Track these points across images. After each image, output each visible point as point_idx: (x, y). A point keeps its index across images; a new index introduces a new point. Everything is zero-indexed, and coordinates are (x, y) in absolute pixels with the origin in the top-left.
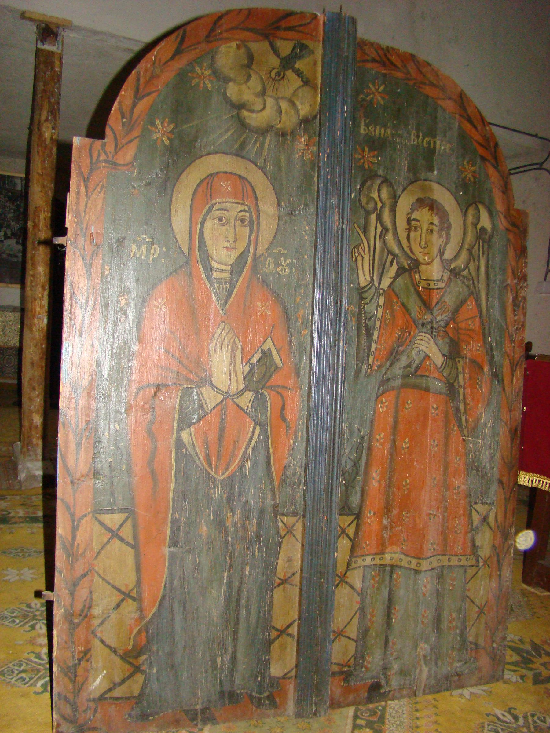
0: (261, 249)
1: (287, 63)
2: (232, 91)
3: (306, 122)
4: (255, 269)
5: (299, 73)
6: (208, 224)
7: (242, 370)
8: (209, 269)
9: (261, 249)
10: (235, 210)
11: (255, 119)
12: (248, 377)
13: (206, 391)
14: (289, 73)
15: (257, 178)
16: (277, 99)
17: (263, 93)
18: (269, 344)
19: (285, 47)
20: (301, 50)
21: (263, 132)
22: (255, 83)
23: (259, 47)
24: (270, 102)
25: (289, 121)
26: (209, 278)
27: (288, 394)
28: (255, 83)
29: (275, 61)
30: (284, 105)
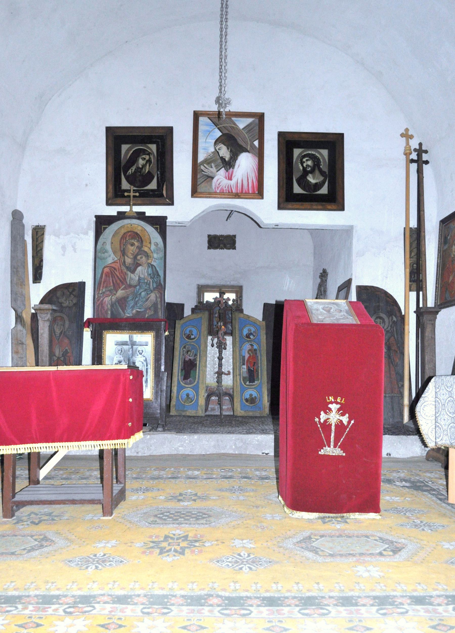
0: (66, 329)
1: (71, 293)
2: (60, 300)
3: (74, 304)
4: (64, 334)
5: (73, 295)
6: (55, 326)
7: (61, 353)
8: (55, 335)
9: (66, 329)
10: (60, 323)
11: (64, 305)
12: (63, 354)
13: (54, 357)
14: (72, 295)
15: (65, 317)
16: (69, 301)
17: (66, 300)
18: (67, 348)
19: (71, 290)
20: (74, 290)
21: (67, 307)
22: (64, 298)
23: (66, 291)
24: (67, 301)
25: (71, 304)
26: (56, 336)
27: (71, 358)
28: (64, 298)
29: (69, 293)
30: (70, 302)
